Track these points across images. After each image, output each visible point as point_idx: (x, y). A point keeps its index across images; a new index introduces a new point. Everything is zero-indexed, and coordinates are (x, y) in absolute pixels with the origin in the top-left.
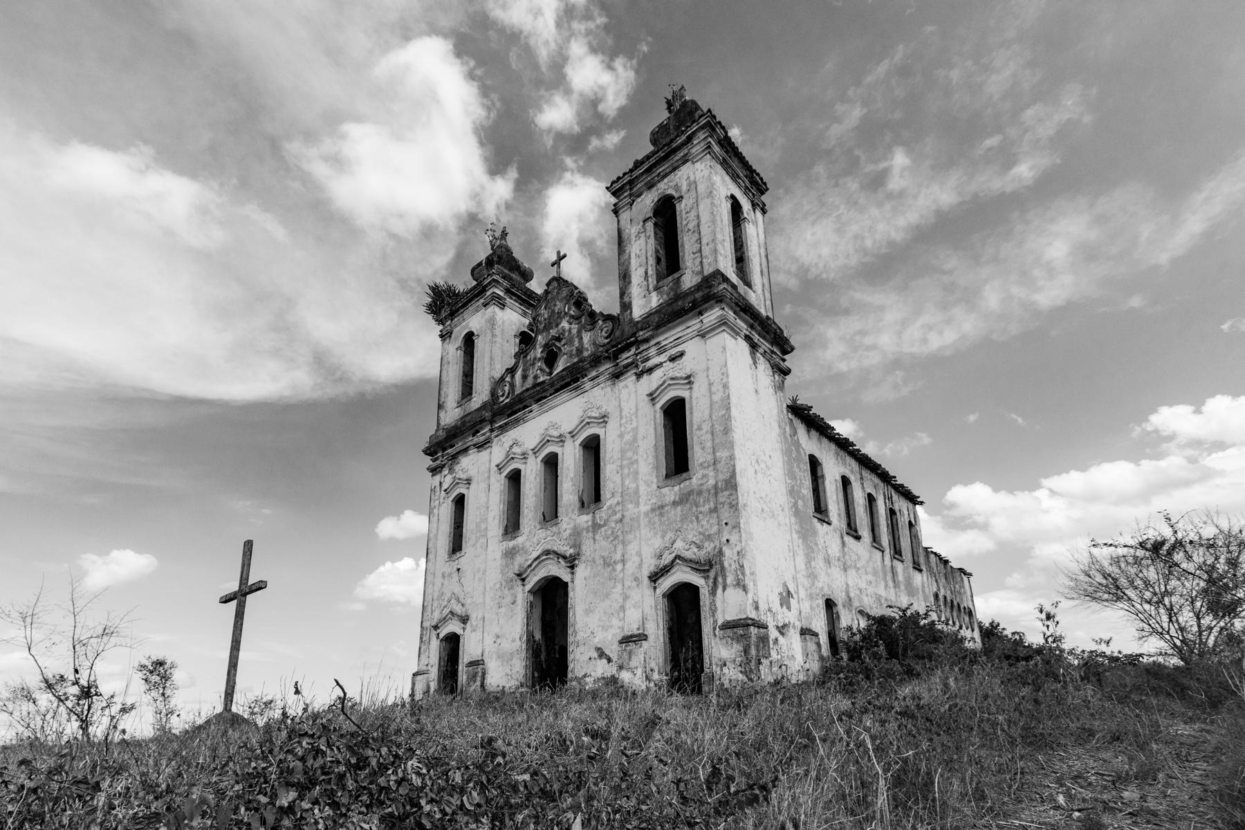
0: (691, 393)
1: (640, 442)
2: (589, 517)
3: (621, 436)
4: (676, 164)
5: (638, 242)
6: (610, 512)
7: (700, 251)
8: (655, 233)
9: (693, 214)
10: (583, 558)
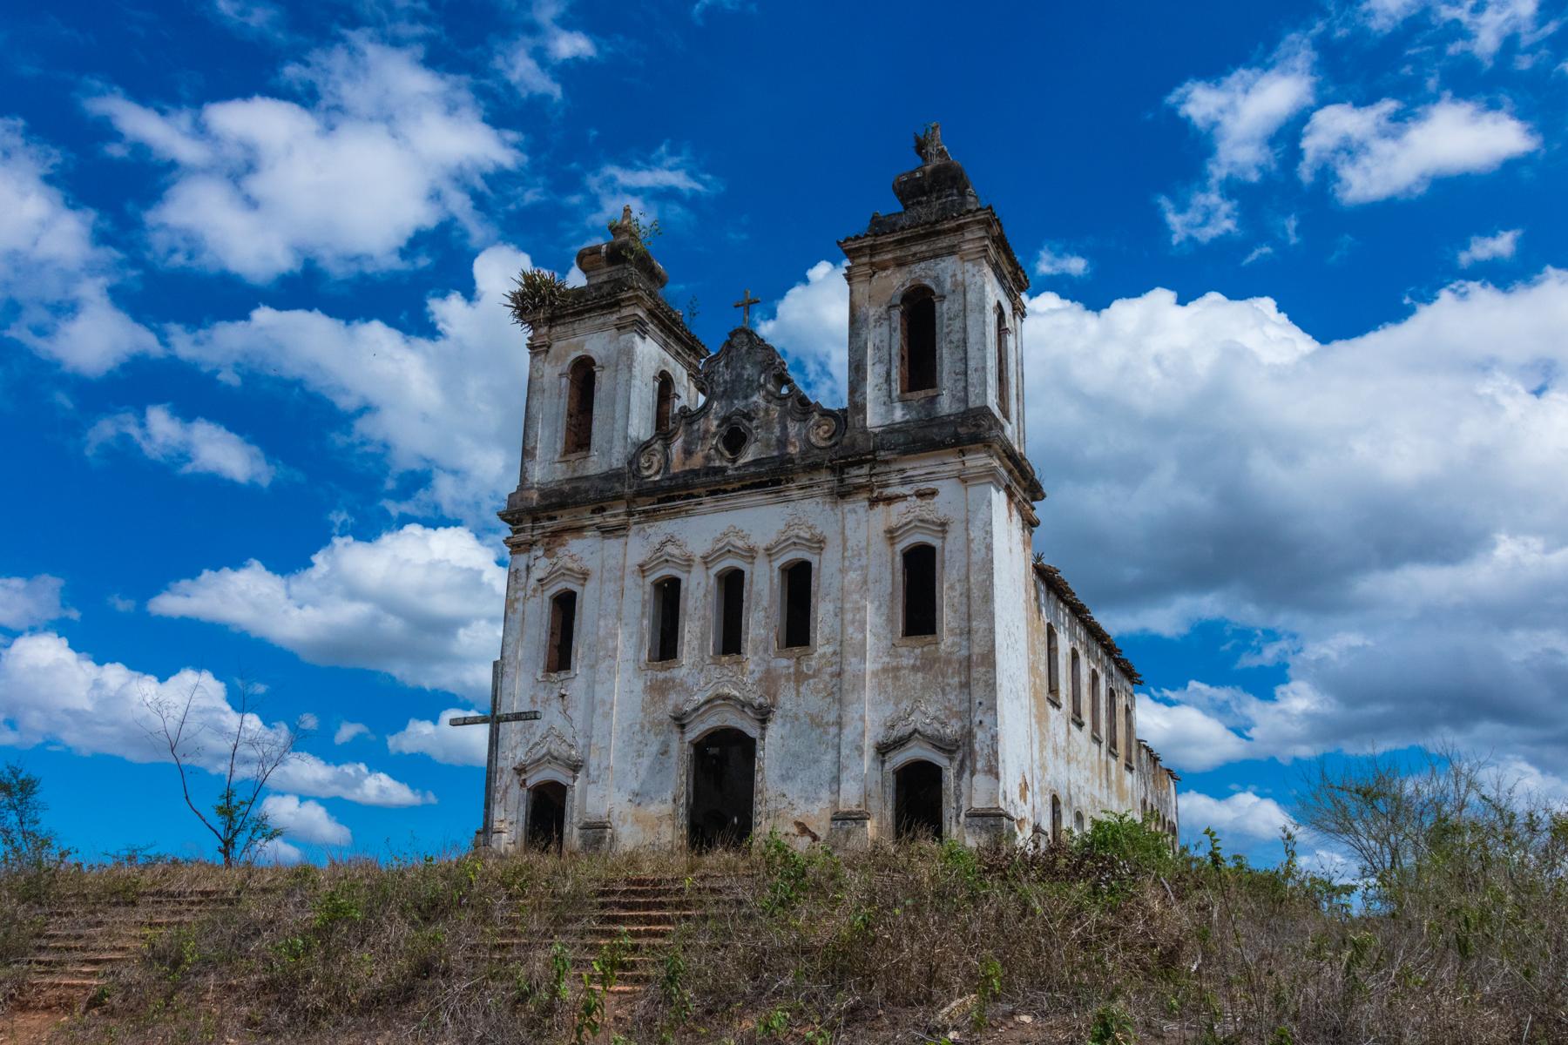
0: (943, 542)
1: (871, 586)
2: (792, 662)
4: (940, 252)
5: (878, 330)
6: (823, 661)
7: (966, 374)
8: (902, 325)
9: (957, 324)
10: (779, 712)
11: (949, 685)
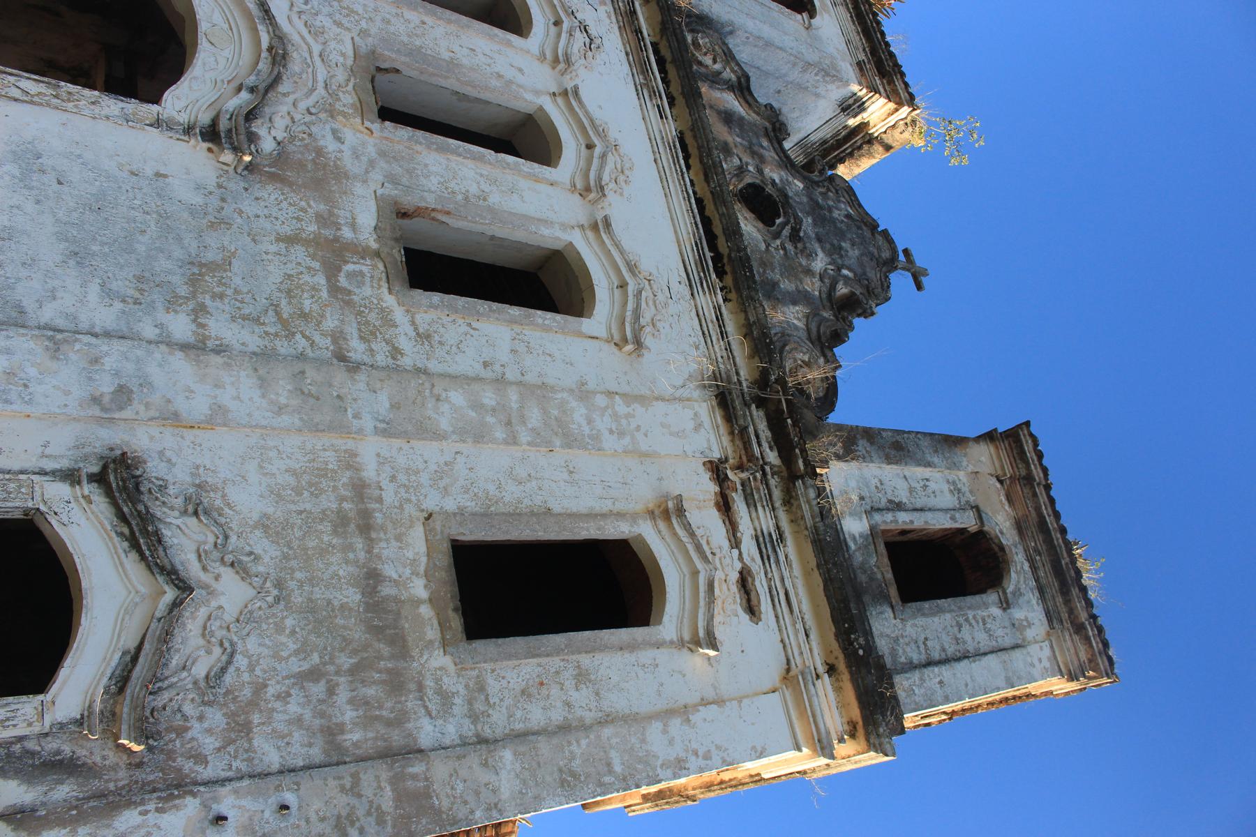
0: (672, 642)
3: (583, 393)
4: (1048, 596)
6: (372, 317)
11: (331, 691)
